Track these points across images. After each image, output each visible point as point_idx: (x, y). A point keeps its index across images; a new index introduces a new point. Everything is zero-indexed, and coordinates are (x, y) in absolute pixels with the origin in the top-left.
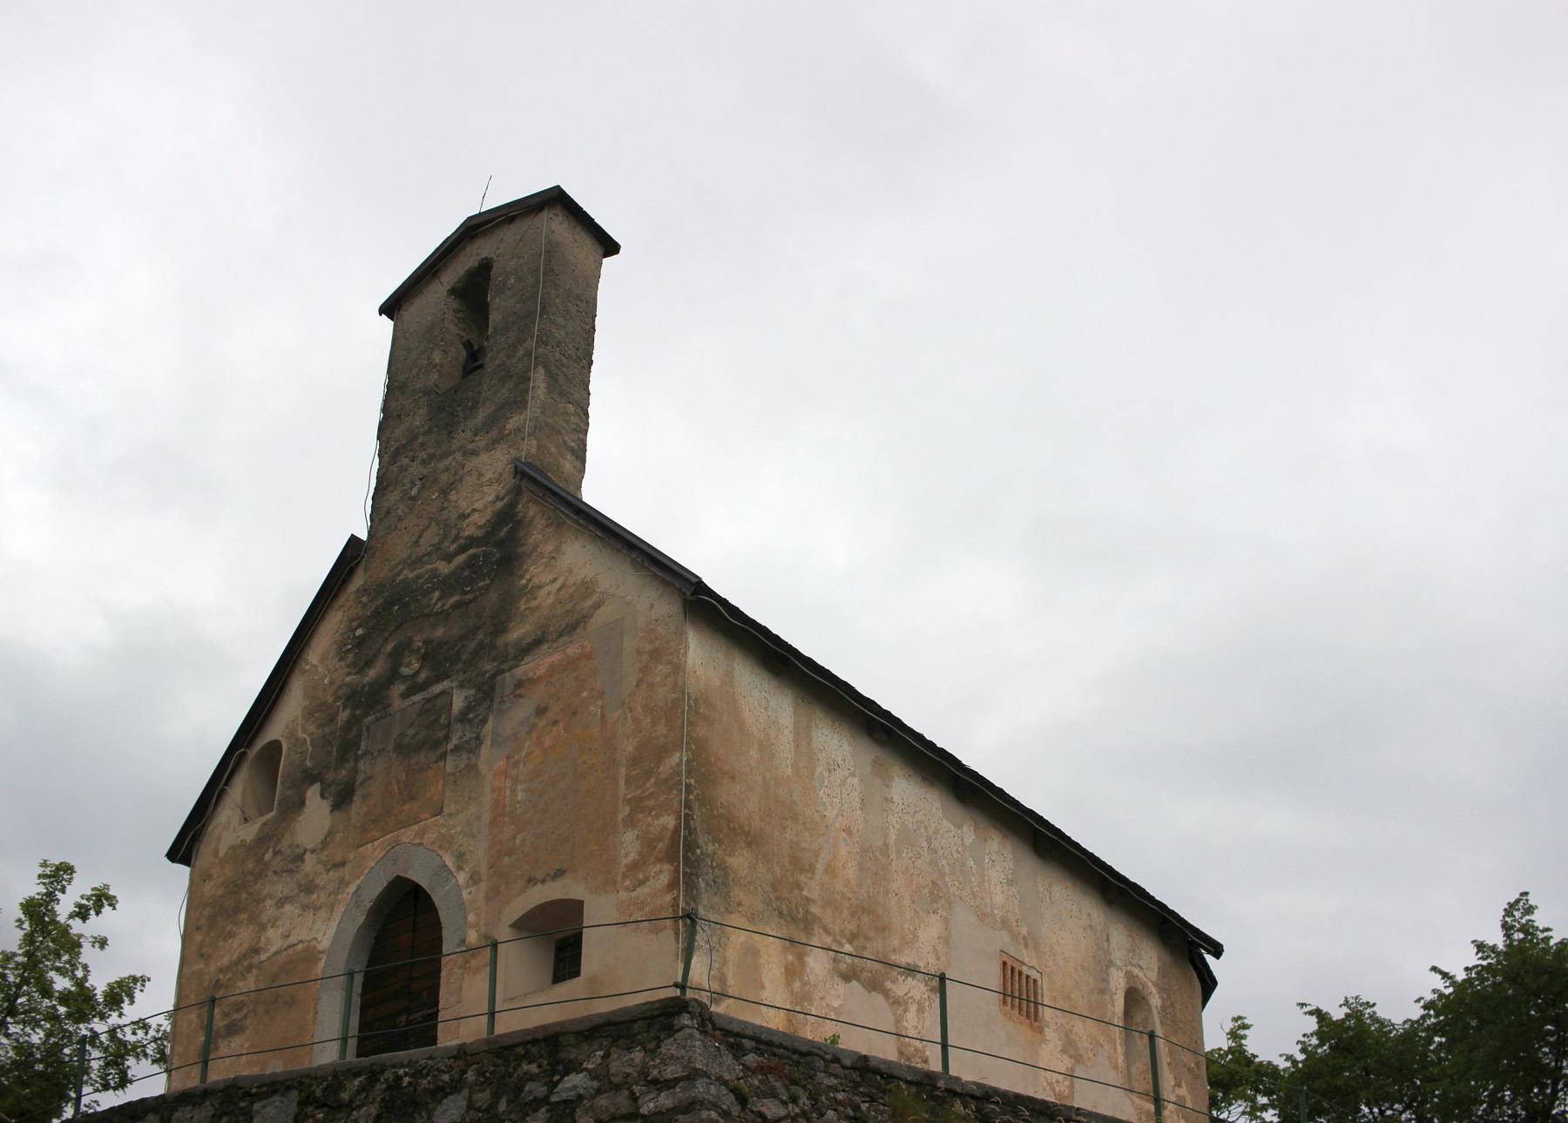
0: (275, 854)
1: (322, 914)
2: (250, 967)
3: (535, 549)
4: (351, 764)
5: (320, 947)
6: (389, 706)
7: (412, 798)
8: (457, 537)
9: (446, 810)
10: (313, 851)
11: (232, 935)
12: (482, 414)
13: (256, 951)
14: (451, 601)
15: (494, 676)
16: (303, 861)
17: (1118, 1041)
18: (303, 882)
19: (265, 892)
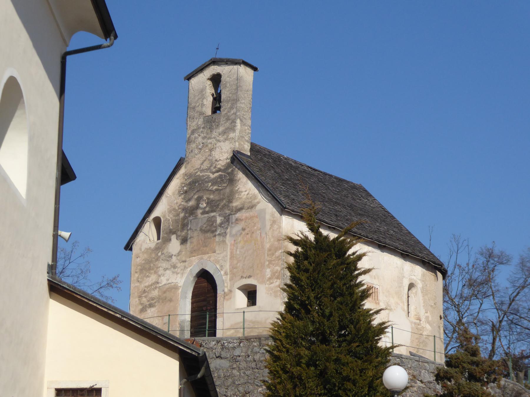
0: (162, 254)
1: (179, 275)
2: (156, 288)
3: (240, 179)
4: (185, 231)
5: (179, 285)
6: (197, 216)
7: (206, 246)
8: (215, 167)
9: (217, 252)
10: (175, 256)
11: (148, 276)
12: (221, 129)
13: (158, 283)
14: (215, 187)
15: (229, 215)
16: (172, 258)
18: (172, 265)
19: (159, 265)
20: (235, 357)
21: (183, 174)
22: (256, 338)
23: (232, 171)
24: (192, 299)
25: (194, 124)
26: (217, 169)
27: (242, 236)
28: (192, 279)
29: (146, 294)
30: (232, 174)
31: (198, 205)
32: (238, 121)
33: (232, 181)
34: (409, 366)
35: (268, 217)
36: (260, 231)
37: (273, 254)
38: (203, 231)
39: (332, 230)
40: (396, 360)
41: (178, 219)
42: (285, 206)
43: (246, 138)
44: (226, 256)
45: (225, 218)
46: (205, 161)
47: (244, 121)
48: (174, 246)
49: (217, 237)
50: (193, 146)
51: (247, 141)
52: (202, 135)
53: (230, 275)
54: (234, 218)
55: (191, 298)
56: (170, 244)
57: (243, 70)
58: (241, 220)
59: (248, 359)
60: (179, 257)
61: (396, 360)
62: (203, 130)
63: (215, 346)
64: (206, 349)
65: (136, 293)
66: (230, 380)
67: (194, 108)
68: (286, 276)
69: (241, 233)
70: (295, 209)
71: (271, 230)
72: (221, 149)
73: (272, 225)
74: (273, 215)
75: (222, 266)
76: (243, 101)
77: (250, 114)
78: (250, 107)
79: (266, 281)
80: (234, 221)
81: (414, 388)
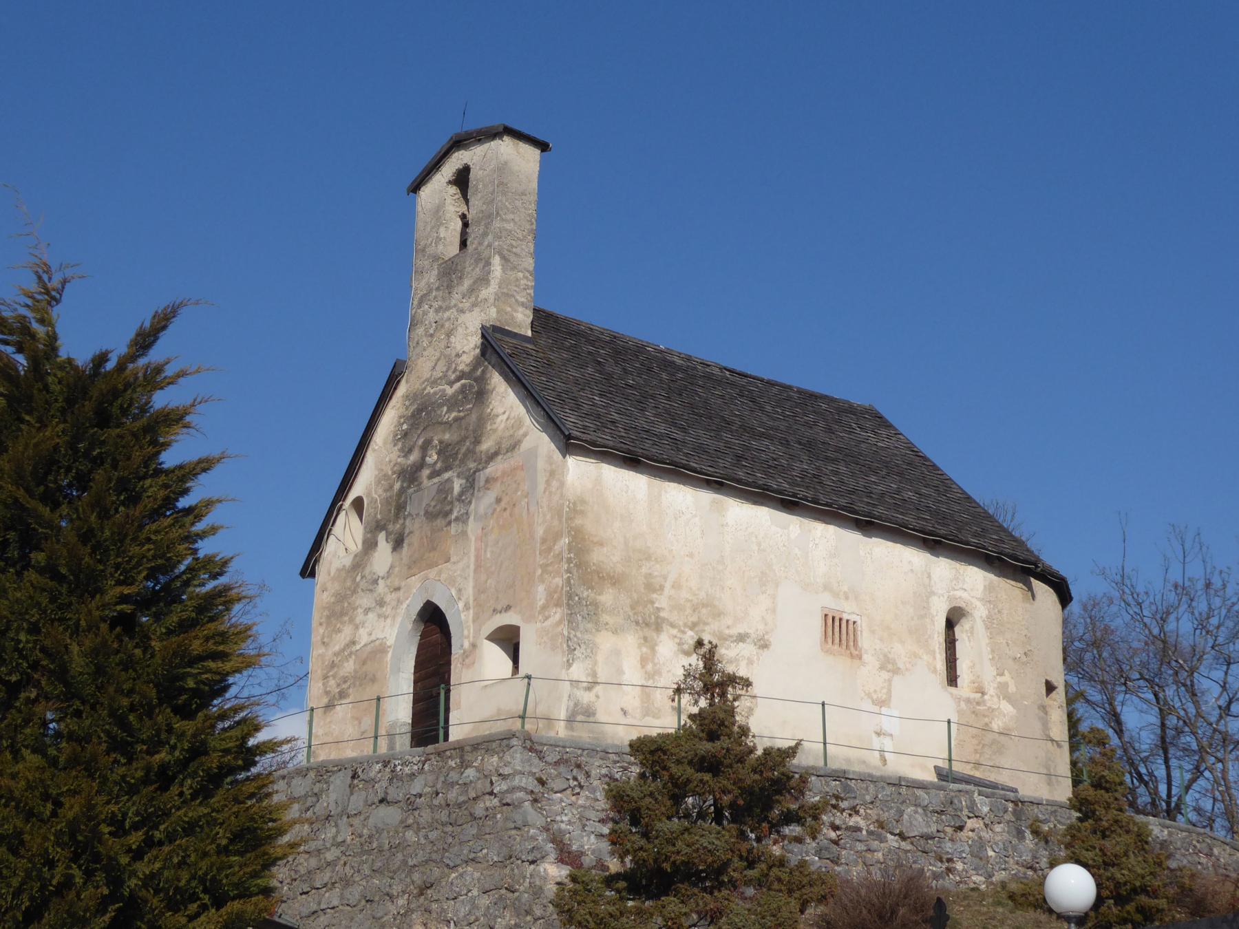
0: (362, 577)
1: (389, 621)
2: (350, 655)
3: (494, 389)
4: (401, 521)
5: (388, 644)
6: (421, 483)
7: (434, 549)
8: (455, 370)
9: (452, 560)
10: (383, 578)
11: (339, 631)
12: (467, 283)
13: (353, 643)
14: (454, 414)
15: (475, 472)
16: (378, 584)
17: (937, 651)
18: (378, 599)
19: (357, 604)
20: (413, 799)
21: (403, 396)
22: (455, 749)
23: (483, 372)
24: (415, 673)
25: (423, 283)
26: (458, 373)
27: (495, 516)
28: (410, 626)
29: (336, 669)
30: (482, 380)
31: (423, 458)
32: (496, 261)
33: (481, 395)
34: (868, 798)
35: (541, 464)
36: (526, 500)
37: (550, 549)
38: (430, 516)
39: (718, 489)
40: (828, 786)
41: (390, 497)
42: (567, 433)
43: (518, 297)
44: (468, 567)
45: (467, 480)
46: (438, 360)
47: (512, 260)
48: (383, 555)
49: (453, 525)
50: (420, 331)
51: (523, 304)
52: (436, 305)
53: (474, 608)
54: (481, 477)
55: (413, 671)
56: (376, 554)
57: (505, 147)
58: (495, 480)
59: (436, 802)
60: (390, 580)
61: (828, 786)
62: (437, 293)
63: (379, 775)
64: (363, 782)
65: (319, 671)
66: (400, 856)
67: (423, 250)
68: (577, 598)
69: (495, 510)
70: (599, 440)
71: (547, 493)
72: (466, 327)
73: (548, 483)
74: (550, 457)
75: (460, 591)
76: (511, 216)
77: (531, 246)
78: (531, 231)
79: (537, 614)
80: (482, 483)
81: (876, 854)
